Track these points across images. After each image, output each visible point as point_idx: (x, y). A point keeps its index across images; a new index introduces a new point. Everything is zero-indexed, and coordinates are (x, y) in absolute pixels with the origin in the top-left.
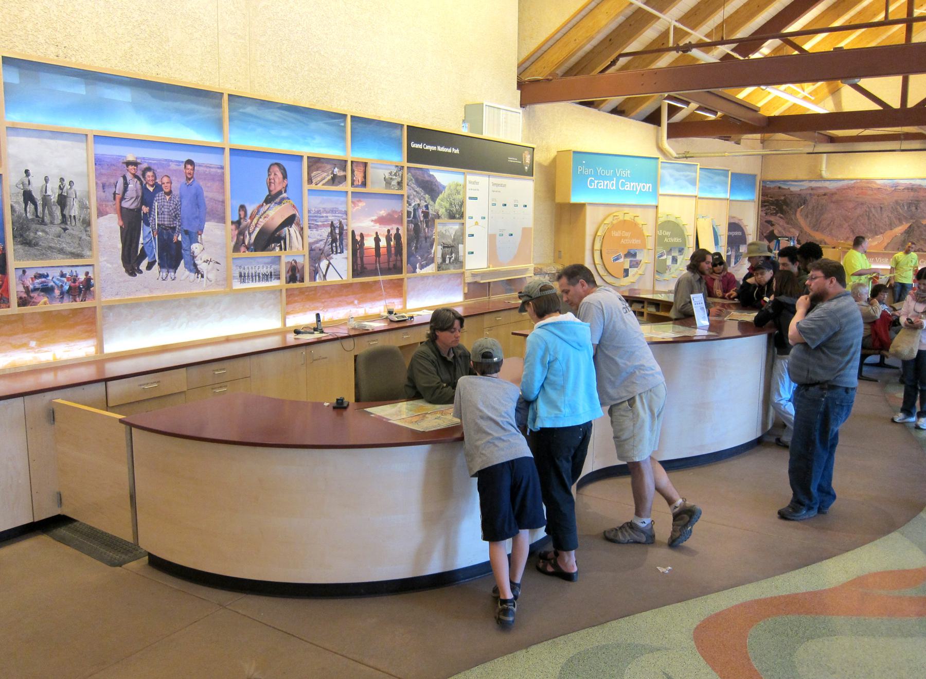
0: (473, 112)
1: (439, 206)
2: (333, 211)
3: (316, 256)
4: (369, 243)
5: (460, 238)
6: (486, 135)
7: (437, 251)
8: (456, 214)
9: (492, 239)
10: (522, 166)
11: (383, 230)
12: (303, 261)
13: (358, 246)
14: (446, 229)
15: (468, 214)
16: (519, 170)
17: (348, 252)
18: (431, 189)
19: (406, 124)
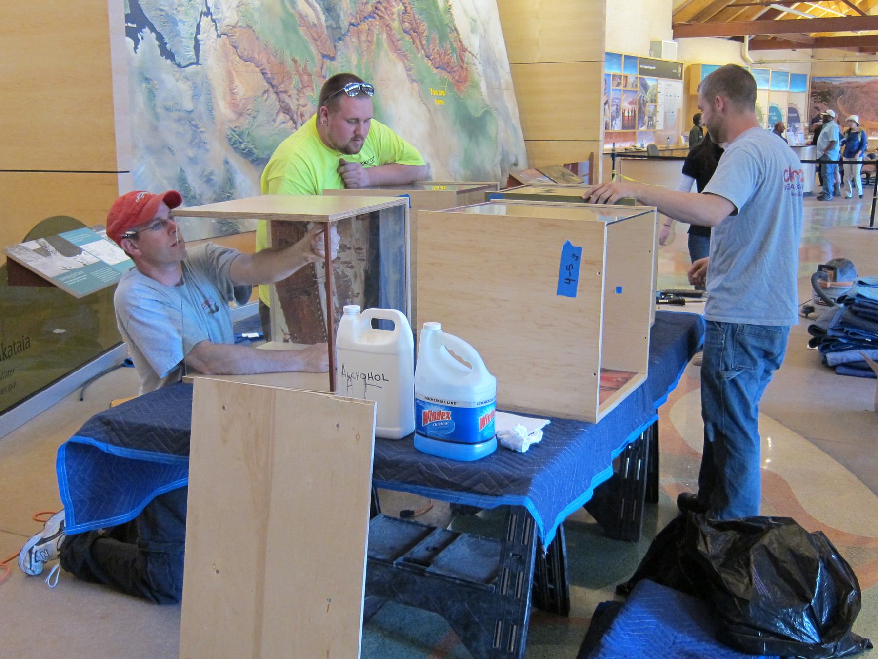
0: (655, 46)
1: (648, 97)
2: (617, 98)
3: (613, 118)
4: (626, 114)
5: (655, 112)
6: (664, 58)
7: (646, 118)
8: (654, 101)
9: (665, 113)
10: (677, 74)
11: (630, 107)
12: (609, 120)
13: (624, 114)
14: (649, 108)
15: (658, 100)
16: (676, 77)
17: (621, 118)
18: (645, 87)
19: (639, 56)
